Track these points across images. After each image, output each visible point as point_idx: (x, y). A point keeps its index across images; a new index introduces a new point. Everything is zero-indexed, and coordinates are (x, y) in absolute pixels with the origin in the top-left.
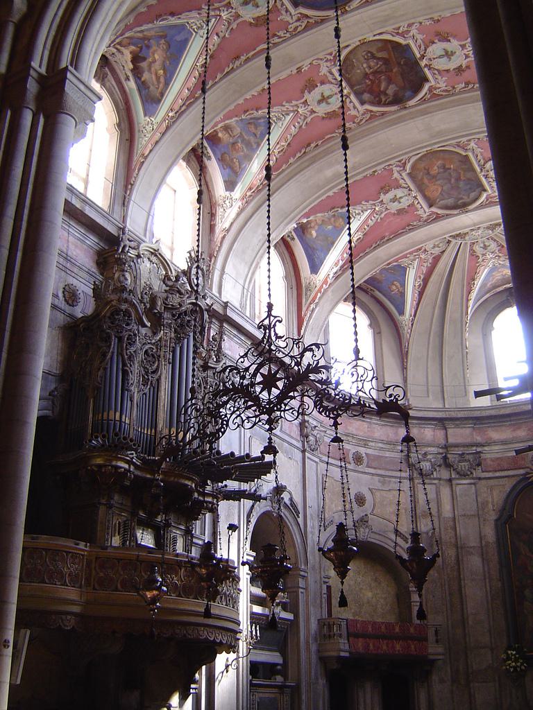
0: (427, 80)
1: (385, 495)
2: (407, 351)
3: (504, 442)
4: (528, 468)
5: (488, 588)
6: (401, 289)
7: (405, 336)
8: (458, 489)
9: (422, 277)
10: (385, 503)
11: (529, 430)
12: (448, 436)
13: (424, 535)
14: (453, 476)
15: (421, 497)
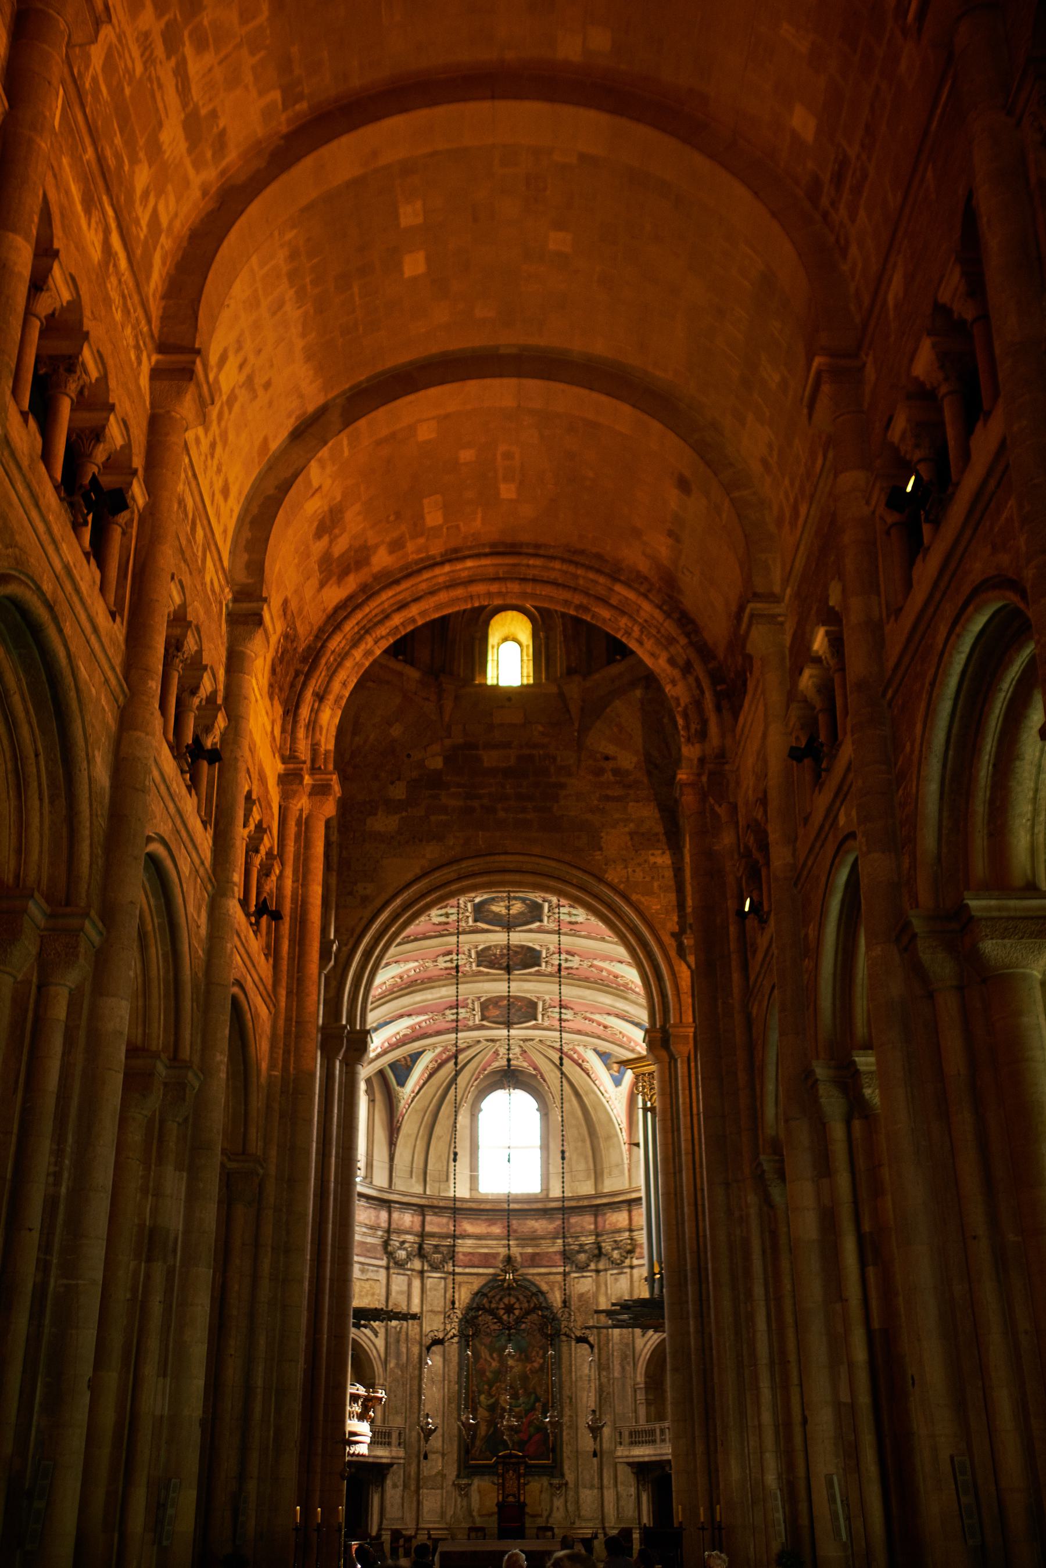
0: (539, 965)
1: (363, 1285)
2: (400, 1127)
3: (478, 1237)
4: (497, 1267)
5: (446, 1390)
6: (409, 1063)
7: (400, 1109)
8: (429, 1283)
9: (439, 1061)
10: (363, 1293)
11: (504, 1227)
12: (426, 1224)
13: (393, 1330)
14: (426, 1268)
15: (394, 1288)
